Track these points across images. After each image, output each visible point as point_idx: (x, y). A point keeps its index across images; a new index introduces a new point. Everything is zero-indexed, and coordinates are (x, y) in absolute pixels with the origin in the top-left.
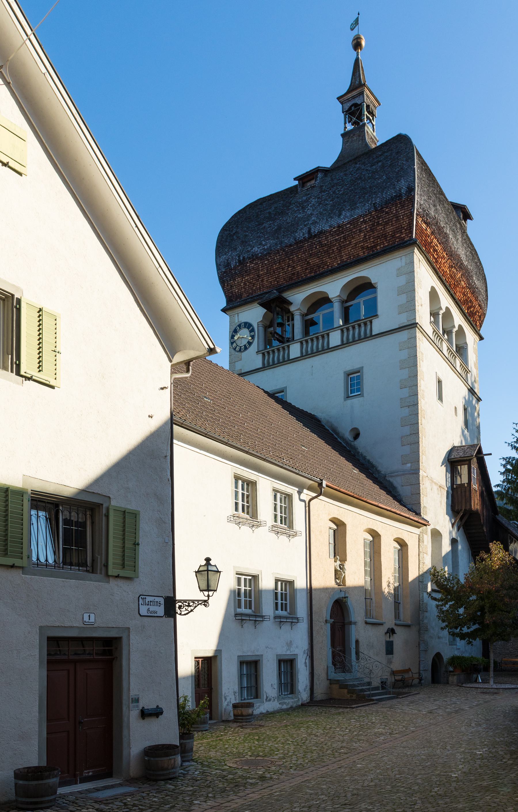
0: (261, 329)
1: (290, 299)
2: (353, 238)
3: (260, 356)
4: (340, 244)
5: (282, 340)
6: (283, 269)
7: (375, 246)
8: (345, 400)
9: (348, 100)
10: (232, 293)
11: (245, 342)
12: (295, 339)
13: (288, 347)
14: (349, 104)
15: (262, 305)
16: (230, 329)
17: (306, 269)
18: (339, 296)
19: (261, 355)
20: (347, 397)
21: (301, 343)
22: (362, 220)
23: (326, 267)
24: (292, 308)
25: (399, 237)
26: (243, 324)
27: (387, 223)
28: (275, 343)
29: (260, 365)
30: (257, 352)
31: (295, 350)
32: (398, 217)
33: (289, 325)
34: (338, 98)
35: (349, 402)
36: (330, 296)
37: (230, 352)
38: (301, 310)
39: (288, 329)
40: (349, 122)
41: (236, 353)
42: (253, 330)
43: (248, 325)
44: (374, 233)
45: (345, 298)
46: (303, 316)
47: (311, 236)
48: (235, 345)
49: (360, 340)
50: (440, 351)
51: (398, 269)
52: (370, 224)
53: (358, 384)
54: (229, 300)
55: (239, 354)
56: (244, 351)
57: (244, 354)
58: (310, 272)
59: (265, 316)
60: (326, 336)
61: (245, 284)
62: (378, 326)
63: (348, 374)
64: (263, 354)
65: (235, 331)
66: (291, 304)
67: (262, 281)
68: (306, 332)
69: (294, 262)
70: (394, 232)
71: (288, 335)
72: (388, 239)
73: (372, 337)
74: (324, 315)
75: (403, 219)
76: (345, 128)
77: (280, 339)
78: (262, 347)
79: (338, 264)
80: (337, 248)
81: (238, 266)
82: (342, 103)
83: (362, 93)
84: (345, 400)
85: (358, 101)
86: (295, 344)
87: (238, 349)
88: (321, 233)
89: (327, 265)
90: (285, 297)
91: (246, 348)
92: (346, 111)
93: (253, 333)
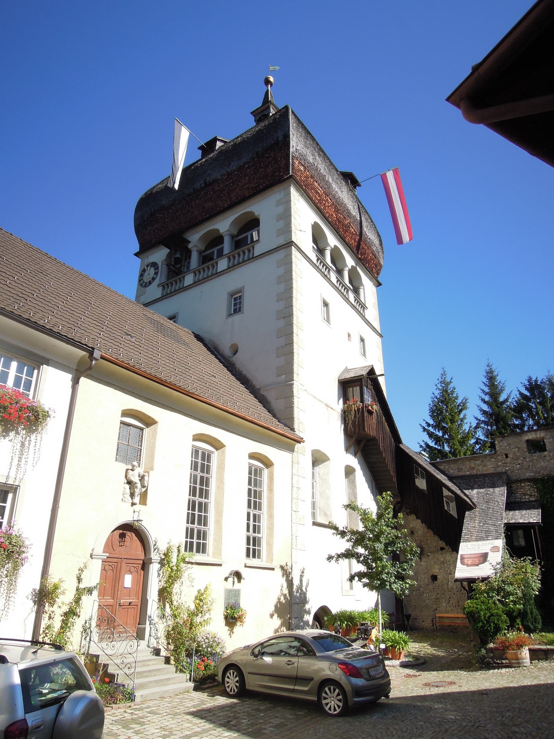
8: (227, 318)
9: (259, 113)
14: (259, 116)
19: (161, 287)
20: (229, 315)
24: (190, 246)
34: (252, 113)
35: (231, 319)
38: (197, 247)
46: (200, 252)
47: (207, 185)
48: (142, 281)
50: (329, 280)
53: (240, 302)
55: (144, 289)
56: (148, 286)
62: (258, 250)
63: (232, 295)
65: (144, 271)
73: (254, 258)
74: (218, 250)
80: (227, 192)
82: (254, 116)
83: (269, 108)
84: (227, 318)
85: (266, 113)
86: (189, 275)
88: (215, 181)
92: (257, 121)
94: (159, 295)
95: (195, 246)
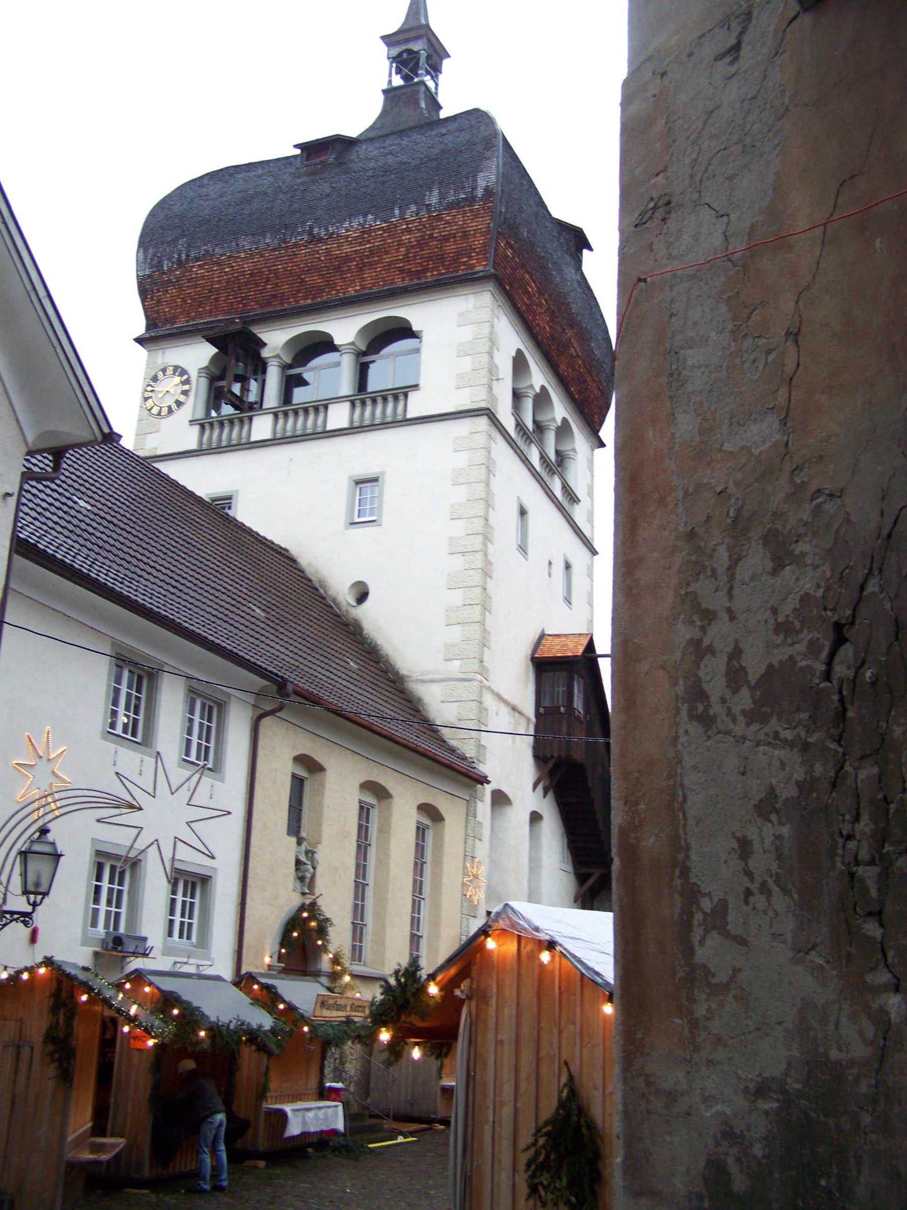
0: (204, 382)
1: (264, 337)
2: (386, 253)
3: (196, 429)
4: (362, 260)
5: (239, 404)
6: (257, 285)
7: (425, 270)
10: (158, 312)
11: (170, 401)
12: (265, 406)
13: (251, 419)
15: (212, 341)
16: (146, 373)
17: (299, 291)
18: (352, 343)
21: (276, 415)
22: (404, 227)
23: (334, 292)
24: (265, 353)
25: (464, 263)
26: (171, 368)
27: (446, 239)
28: (227, 410)
29: (193, 446)
30: (190, 421)
31: (262, 427)
32: (466, 232)
33: (256, 380)
36: (336, 342)
37: (140, 415)
38: (281, 358)
39: (254, 385)
40: (397, 73)
41: (151, 418)
42: (187, 382)
43: (180, 371)
44: (423, 250)
45: (364, 348)
49: (384, 425)
51: (460, 315)
52: (418, 235)
54: (151, 324)
57: (166, 423)
58: (305, 298)
59: (214, 359)
60: (322, 409)
61: (184, 300)
64: (202, 427)
66: (265, 344)
67: (217, 300)
68: (287, 397)
69: (277, 277)
70: (459, 254)
71: (252, 397)
72: (447, 263)
75: (474, 236)
76: (390, 82)
77: (237, 403)
78: (200, 414)
79: (356, 291)
81: (176, 270)
86: (264, 416)
87: (155, 410)
89: (337, 290)
90: (255, 332)
91: (170, 411)
93: (186, 387)
94: (192, 443)
95: (278, 356)
